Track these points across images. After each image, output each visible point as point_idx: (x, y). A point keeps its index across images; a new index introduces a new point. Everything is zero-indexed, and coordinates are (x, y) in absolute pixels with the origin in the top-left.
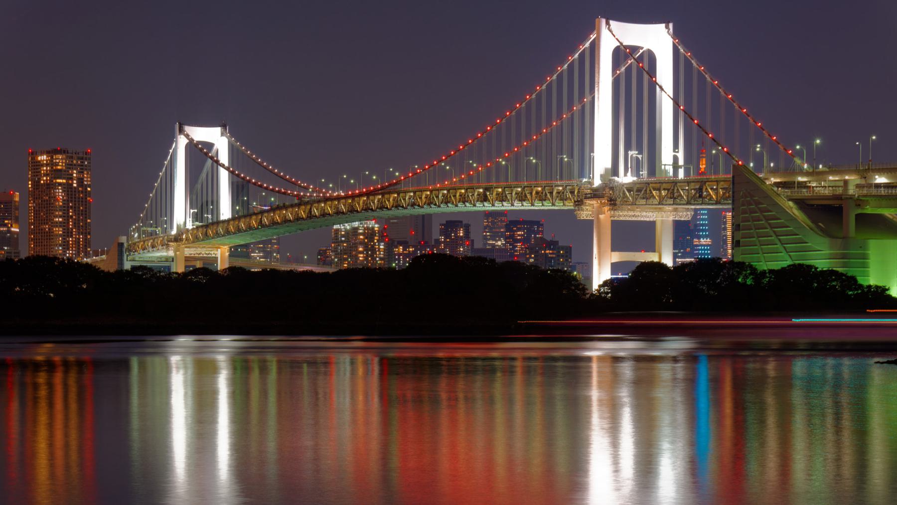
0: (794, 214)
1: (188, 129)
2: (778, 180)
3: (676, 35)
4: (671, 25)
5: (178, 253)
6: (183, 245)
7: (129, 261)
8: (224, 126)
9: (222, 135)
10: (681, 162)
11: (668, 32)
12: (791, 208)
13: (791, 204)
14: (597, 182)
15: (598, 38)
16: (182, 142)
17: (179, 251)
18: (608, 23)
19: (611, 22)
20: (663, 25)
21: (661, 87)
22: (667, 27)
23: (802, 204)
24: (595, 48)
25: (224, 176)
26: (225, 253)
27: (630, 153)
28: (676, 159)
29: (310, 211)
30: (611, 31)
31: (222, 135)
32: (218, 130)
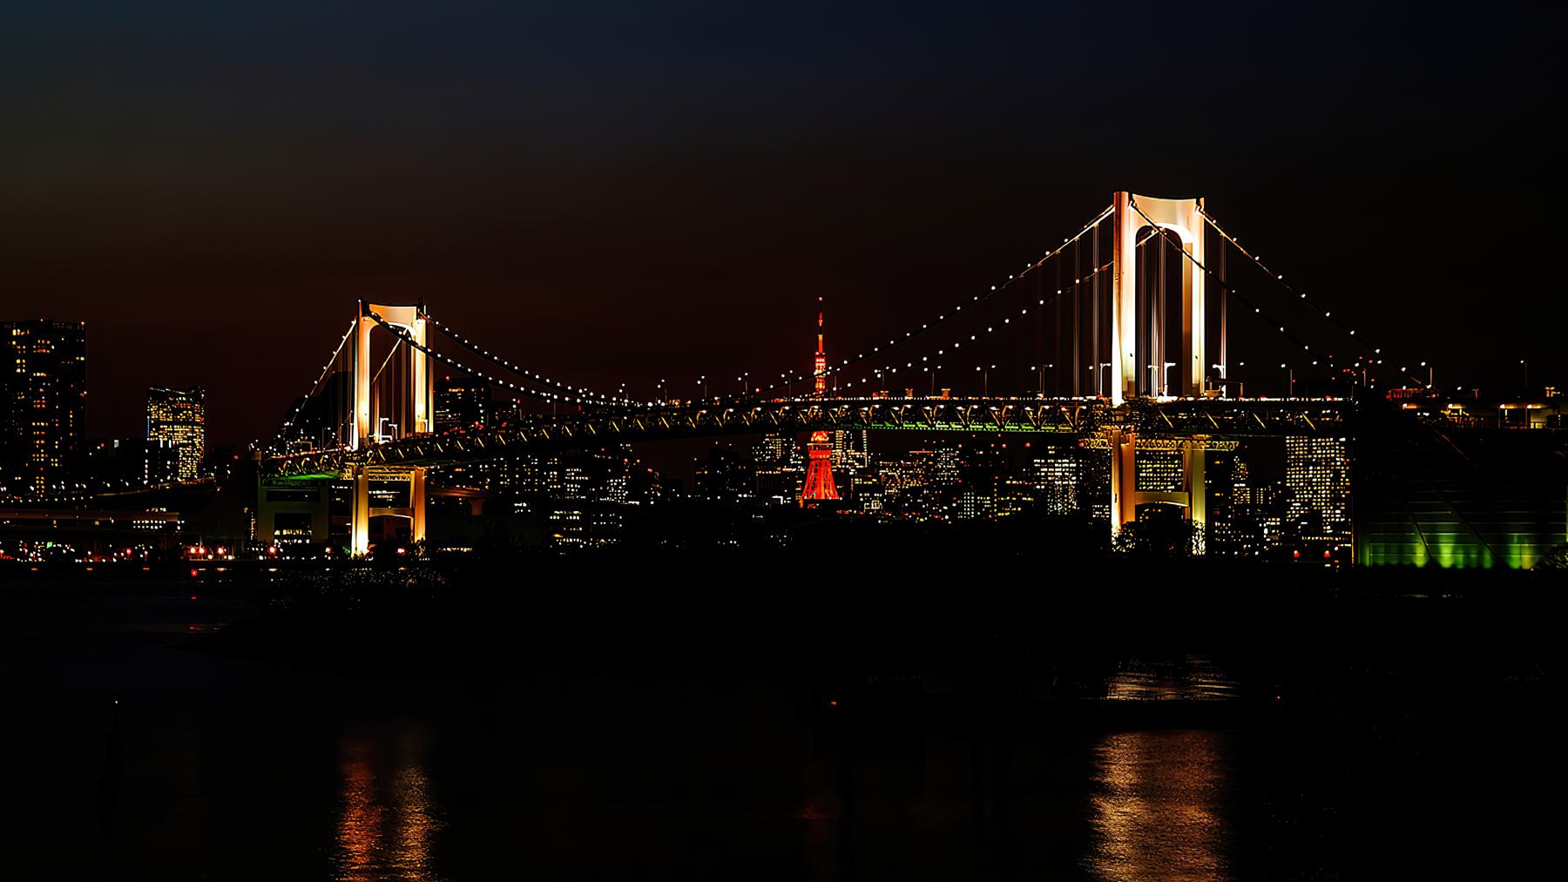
1: (375, 309)
3: (1209, 211)
4: (1202, 200)
5: (360, 476)
6: (367, 465)
7: (265, 485)
8: (420, 307)
9: (419, 316)
10: (1223, 376)
14: (1117, 400)
17: (361, 474)
18: (1131, 198)
19: (1134, 195)
20: (1195, 200)
22: (1198, 203)
24: (1112, 228)
26: (421, 476)
27: (1167, 365)
28: (1211, 373)
30: (1135, 208)
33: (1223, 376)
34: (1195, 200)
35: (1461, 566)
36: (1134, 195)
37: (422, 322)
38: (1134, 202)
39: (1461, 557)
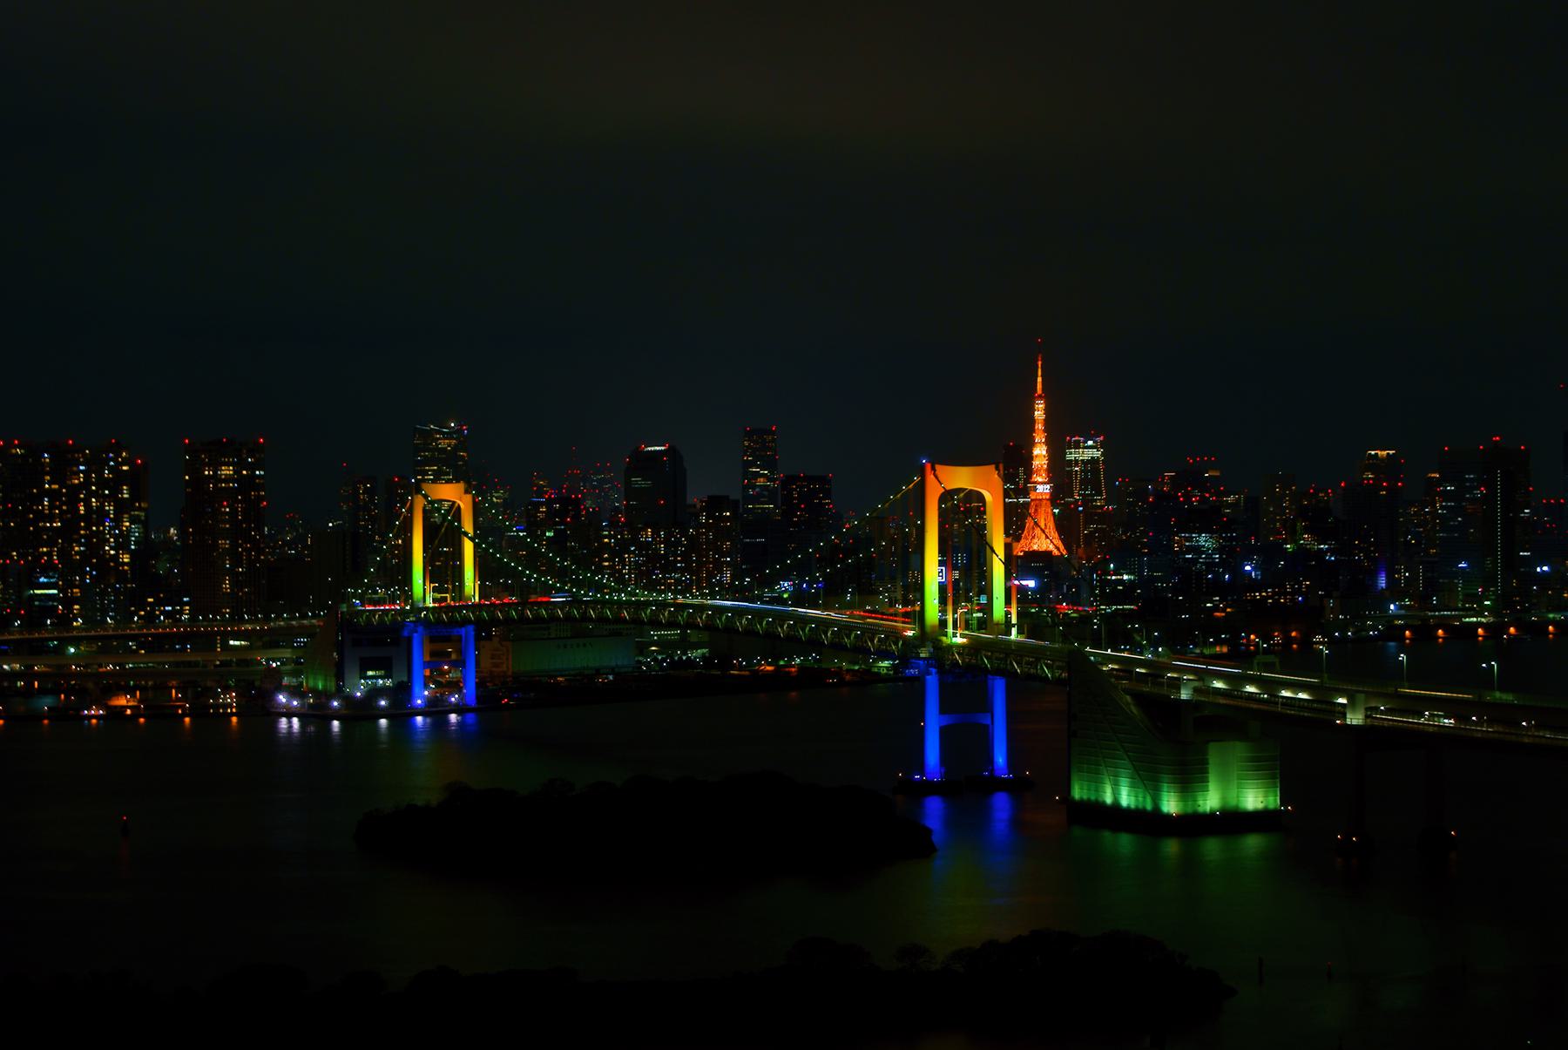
0: (1132, 712)
2: (1116, 667)
9: (467, 492)
10: (1014, 621)
11: (998, 474)
12: (1128, 704)
13: (1128, 698)
15: (922, 486)
16: (419, 503)
17: (416, 632)
18: (933, 469)
19: (937, 467)
20: (993, 466)
21: (993, 551)
22: (997, 469)
23: (1139, 698)
25: (468, 548)
29: (585, 613)
31: (467, 492)
32: (461, 486)
33: (1014, 621)
34: (993, 466)
35: (1133, 806)
36: (937, 467)
37: (468, 498)
38: (935, 471)
39: (1133, 799)
